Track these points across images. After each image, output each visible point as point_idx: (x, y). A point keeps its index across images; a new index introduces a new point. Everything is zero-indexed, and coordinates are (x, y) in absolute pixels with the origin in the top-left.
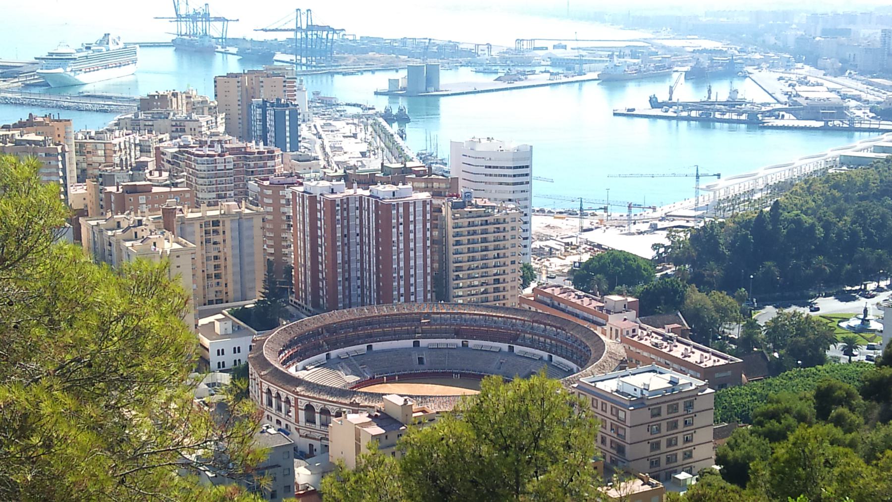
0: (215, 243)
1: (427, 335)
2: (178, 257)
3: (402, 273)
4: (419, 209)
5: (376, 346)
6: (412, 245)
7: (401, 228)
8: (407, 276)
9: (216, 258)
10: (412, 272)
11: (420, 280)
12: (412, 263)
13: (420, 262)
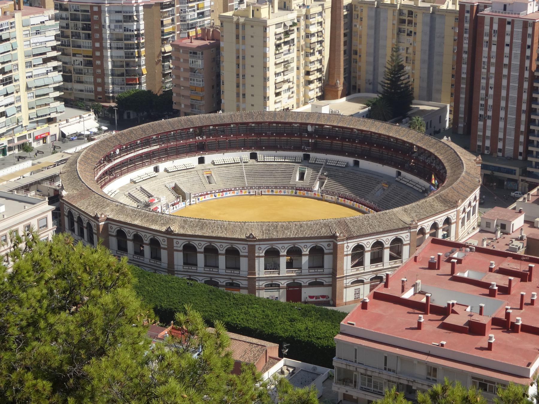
0: (409, 34)
1: (411, 170)
2: (252, 27)
3: (490, 102)
4: (518, 30)
5: (364, 164)
7: (494, 48)
8: (496, 108)
11: (512, 116)
12: (504, 93)
13: (514, 94)
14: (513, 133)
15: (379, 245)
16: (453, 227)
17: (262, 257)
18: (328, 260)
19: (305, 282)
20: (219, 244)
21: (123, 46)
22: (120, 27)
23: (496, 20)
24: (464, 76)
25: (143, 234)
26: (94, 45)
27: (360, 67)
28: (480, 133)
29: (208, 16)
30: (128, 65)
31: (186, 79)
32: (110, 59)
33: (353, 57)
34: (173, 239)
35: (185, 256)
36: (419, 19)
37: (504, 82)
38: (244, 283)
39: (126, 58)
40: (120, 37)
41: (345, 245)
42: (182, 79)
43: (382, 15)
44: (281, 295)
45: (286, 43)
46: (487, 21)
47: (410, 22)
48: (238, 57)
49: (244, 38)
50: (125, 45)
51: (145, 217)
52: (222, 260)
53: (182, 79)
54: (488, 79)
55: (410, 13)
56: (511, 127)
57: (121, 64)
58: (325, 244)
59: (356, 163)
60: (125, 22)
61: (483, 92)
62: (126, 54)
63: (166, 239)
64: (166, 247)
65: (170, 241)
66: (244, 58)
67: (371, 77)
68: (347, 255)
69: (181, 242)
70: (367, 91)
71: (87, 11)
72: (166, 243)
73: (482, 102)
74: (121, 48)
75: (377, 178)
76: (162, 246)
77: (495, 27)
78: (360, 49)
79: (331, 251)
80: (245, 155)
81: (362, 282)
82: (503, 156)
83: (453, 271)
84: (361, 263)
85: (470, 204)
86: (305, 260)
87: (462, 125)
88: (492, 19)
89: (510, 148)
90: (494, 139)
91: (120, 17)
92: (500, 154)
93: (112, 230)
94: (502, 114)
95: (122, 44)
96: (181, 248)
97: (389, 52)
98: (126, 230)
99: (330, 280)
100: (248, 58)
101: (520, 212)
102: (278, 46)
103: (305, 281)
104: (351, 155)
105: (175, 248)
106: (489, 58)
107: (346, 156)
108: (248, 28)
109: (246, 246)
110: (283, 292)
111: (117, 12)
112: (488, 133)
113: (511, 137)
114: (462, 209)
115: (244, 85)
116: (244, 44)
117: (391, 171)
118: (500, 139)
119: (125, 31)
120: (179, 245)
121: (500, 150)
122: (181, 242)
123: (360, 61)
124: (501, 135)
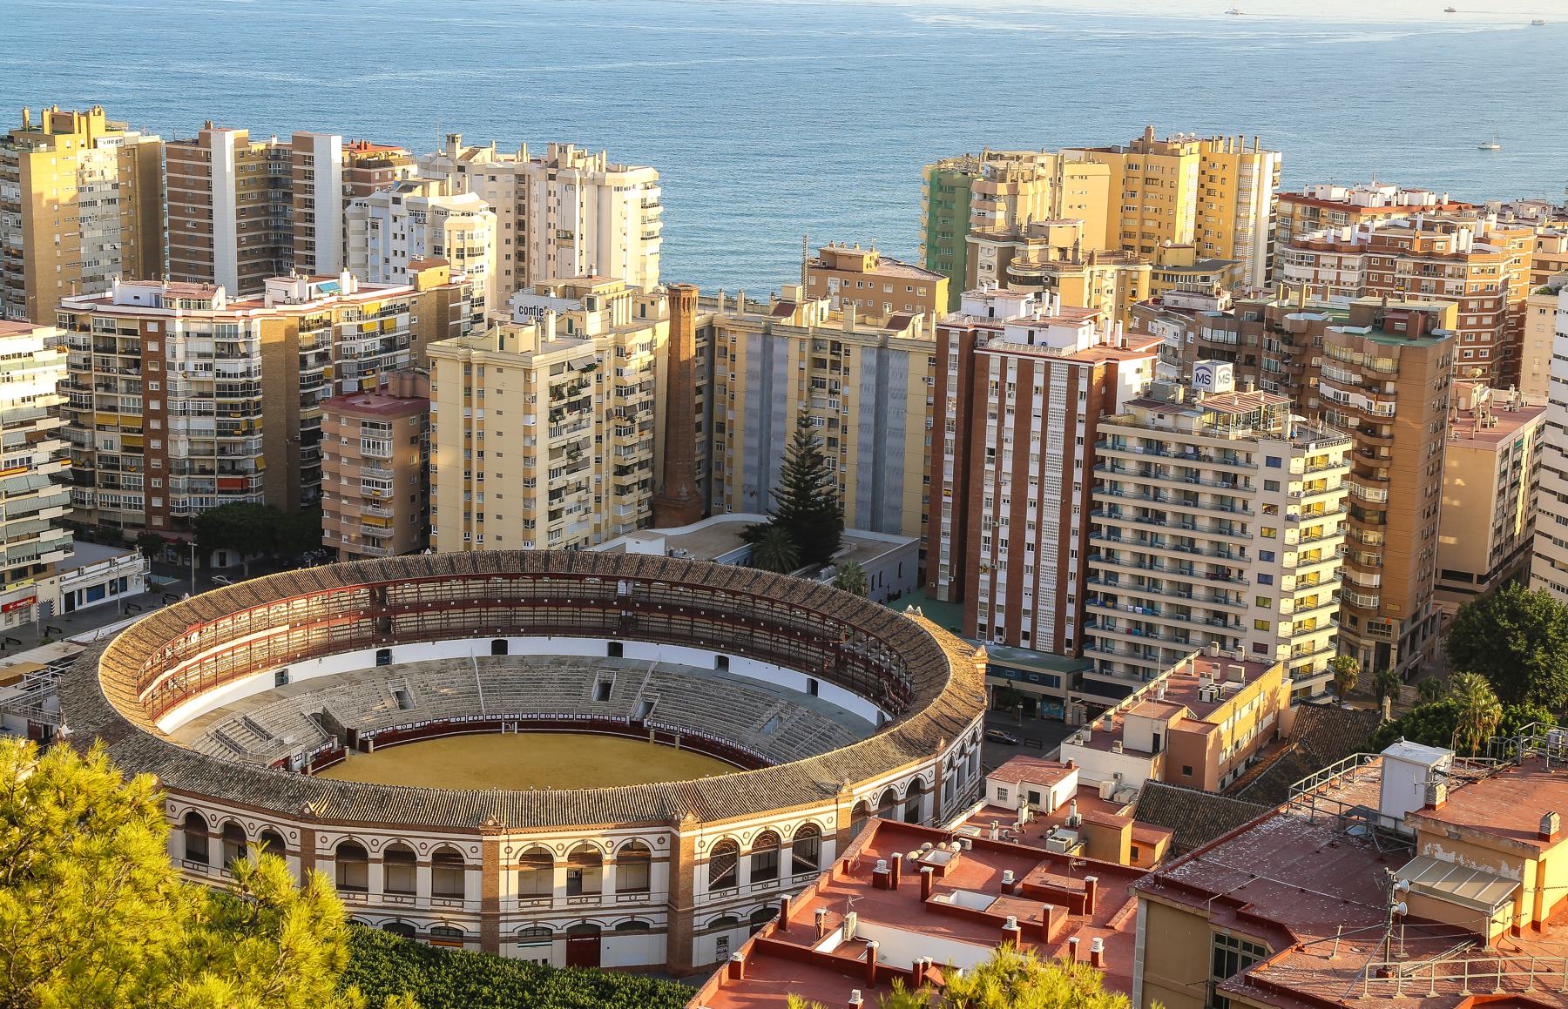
2: (500, 370)
3: (1004, 533)
4: (1059, 383)
5: (741, 666)
6: (1034, 470)
7: (1010, 421)
9: (832, 422)
10: (1030, 537)
12: (1031, 514)
13: (1052, 517)
14: (1053, 598)
15: (769, 839)
16: (929, 799)
17: (514, 867)
18: (658, 873)
19: (607, 923)
20: (417, 842)
21: (214, 409)
22: (208, 367)
23: (1013, 361)
24: (948, 477)
25: (247, 821)
26: (146, 404)
27: (730, 460)
28: (984, 599)
29: (403, 347)
30: (222, 451)
31: (350, 480)
32: (184, 437)
33: (716, 436)
34: (313, 831)
35: (342, 870)
36: (856, 359)
37: (1033, 492)
38: (472, 928)
39: (219, 434)
40: (206, 389)
41: (698, 840)
42: (344, 482)
43: (778, 349)
44: (555, 954)
45: (572, 407)
46: (995, 364)
47: (835, 365)
48: (469, 436)
49: (481, 393)
50: (219, 405)
51: (251, 784)
52: (424, 878)
53: (344, 482)
54: (998, 486)
55: (836, 346)
56: (1048, 585)
57: (208, 447)
58: (653, 839)
59: (723, 663)
60: (219, 356)
61: (988, 512)
62: (219, 426)
63: (298, 831)
64: (298, 849)
65: (308, 837)
66: (481, 435)
67: (754, 481)
68: (701, 862)
69: (332, 837)
70: (747, 509)
71: (134, 332)
72: (298, 841)
73: (987, 534)
74: (211, 414)
75: (768, 694)
76: (288, 847)
77: (1012, 377)
78: (731, 422)
79: (667, 854)
80: (480, 647)
81: (731, 922)
82: (1033, 649)
83: (925, 893)
84: (731, 881)
85: (962, 752)
86: (608, 871)
87: (946, 583)
88: (1004, 361)
89: (1046, 630)
90: (1014, 611)
91: (207, 346)
92: (1025, 644)
93: (175, 815)
94: (1029, 558)
95: (212, 404)
96: (333, 852)
97: (792, 426)
98: (206, 813)
99: (664, 917)
100: (490, 436)
101: (1069, 766)
102: (555, 415)
103: (608, 920)
104: (711, 644)
105: (318, 852)
106: (1000, 441)
107: (701, 647)
108: (490, 372)
109: (479, 845)
110: (560, 947)
111: (199, 335)
112: (1001, 599)
113: (1047, 607)
114: (946, 760)
115: (481, 494)
116: (481, 406)
117: (797, 681)
118: (1026, 612)
119: (218, 375)
120: (327, 845)
121: (1026, 636)
122: (332, 837)
123: (731, 446)
124: (1027, 604)
